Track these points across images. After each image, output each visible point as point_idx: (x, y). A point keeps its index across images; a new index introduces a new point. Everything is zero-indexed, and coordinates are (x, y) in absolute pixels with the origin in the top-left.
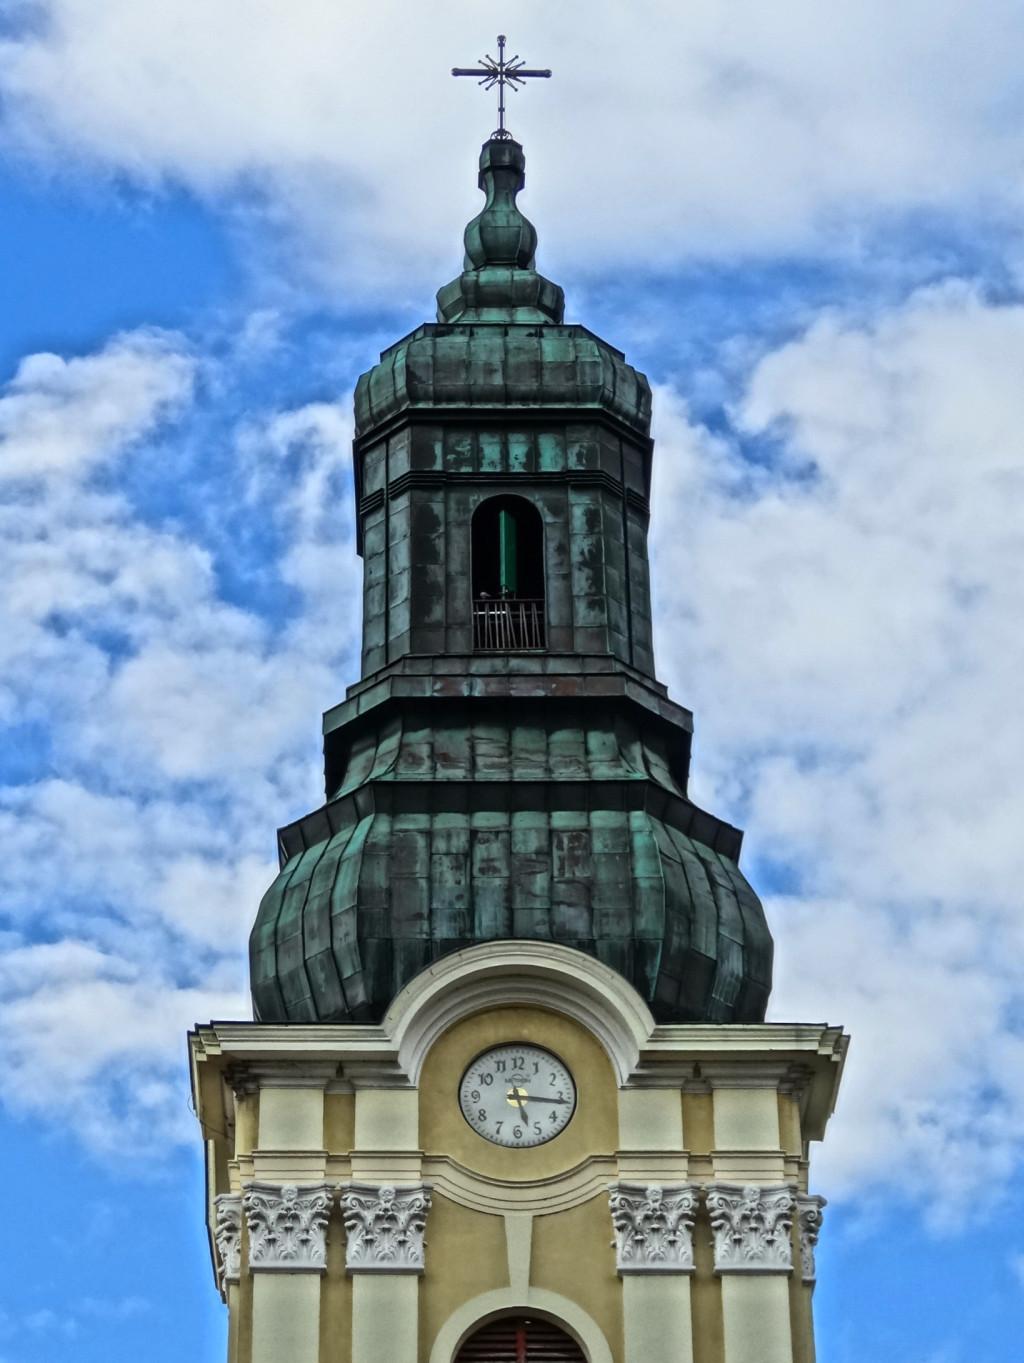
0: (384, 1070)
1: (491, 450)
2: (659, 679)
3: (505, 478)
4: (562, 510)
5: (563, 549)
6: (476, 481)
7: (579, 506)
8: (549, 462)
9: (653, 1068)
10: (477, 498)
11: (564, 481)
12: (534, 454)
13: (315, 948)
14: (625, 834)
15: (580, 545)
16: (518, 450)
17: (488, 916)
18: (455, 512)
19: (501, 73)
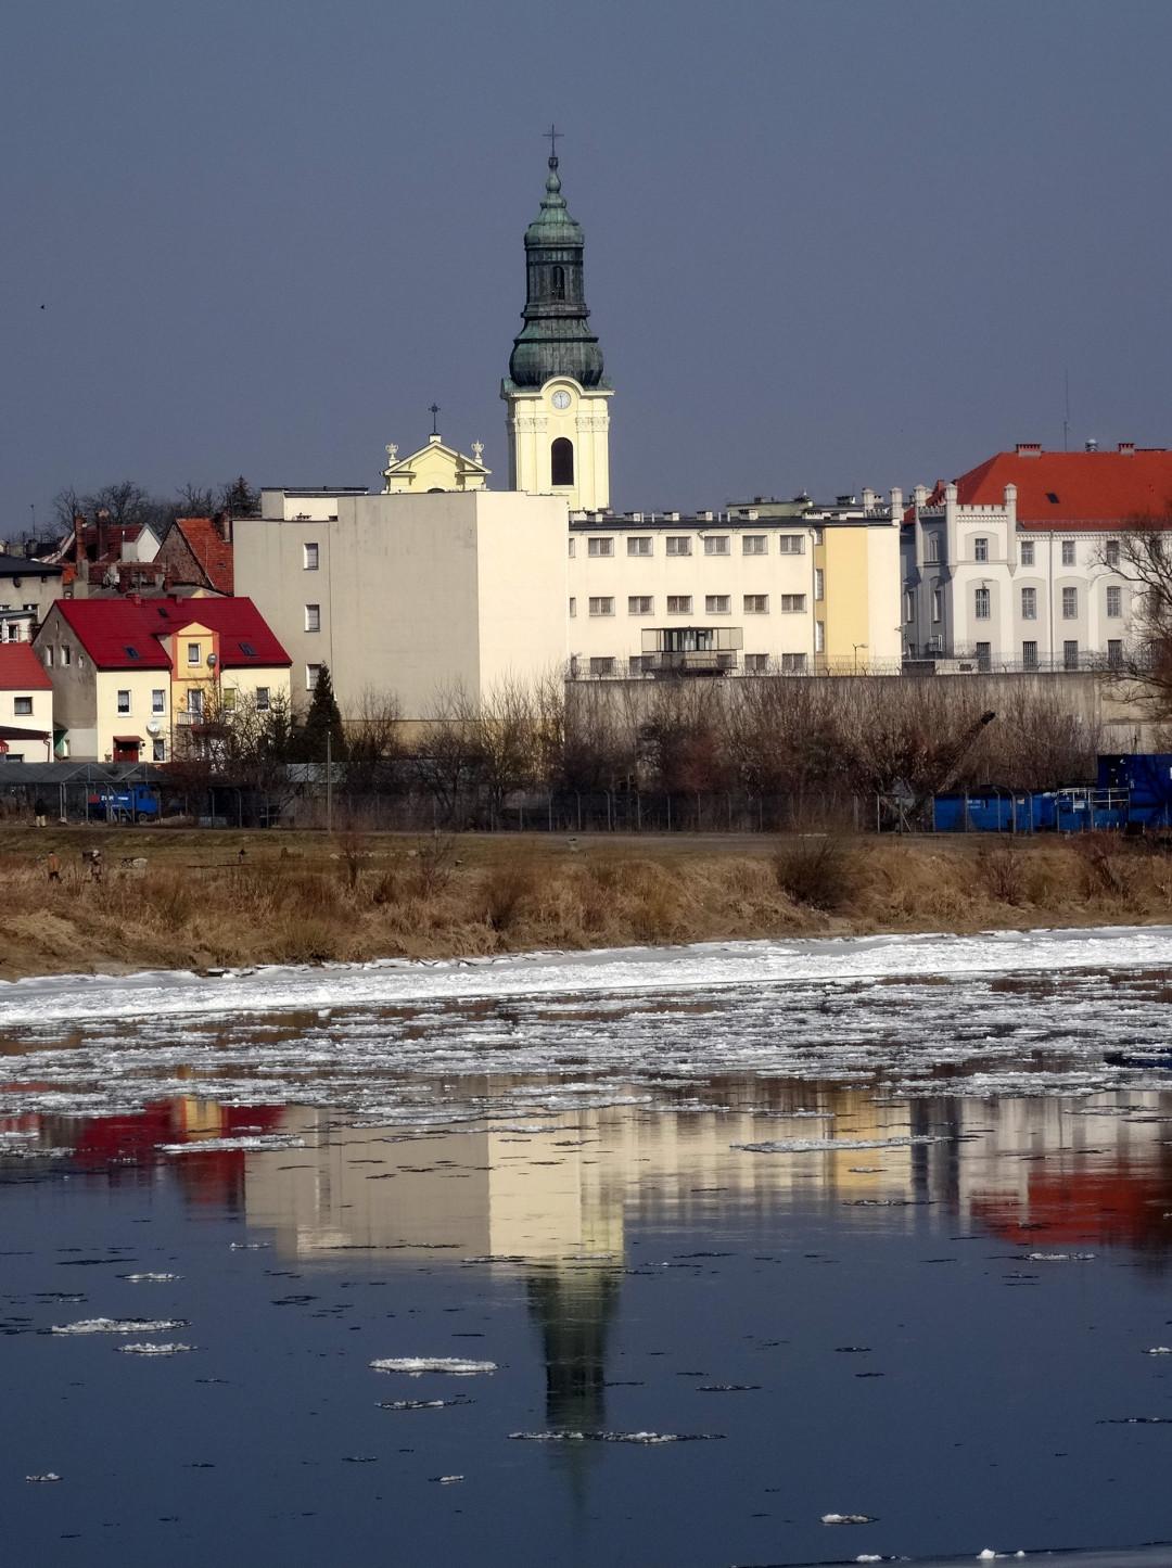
0: (540, 398)
1: (554, 256)
2: (585, 301)
3: (557, 262)
4: (568, 269)
5: (568, 279)
6: (553, 263)
7: (571, 268)
8: (565, 259)
9: (582, 397)
10: (552, 266)
11: (568, 262)
12: (562, 256)
13: (526, 370)
14: (579, 348)
15: (571, 277)
16: (559, 256)
17: (556, 368)
18: (547, 270)
19: (553, 136)
